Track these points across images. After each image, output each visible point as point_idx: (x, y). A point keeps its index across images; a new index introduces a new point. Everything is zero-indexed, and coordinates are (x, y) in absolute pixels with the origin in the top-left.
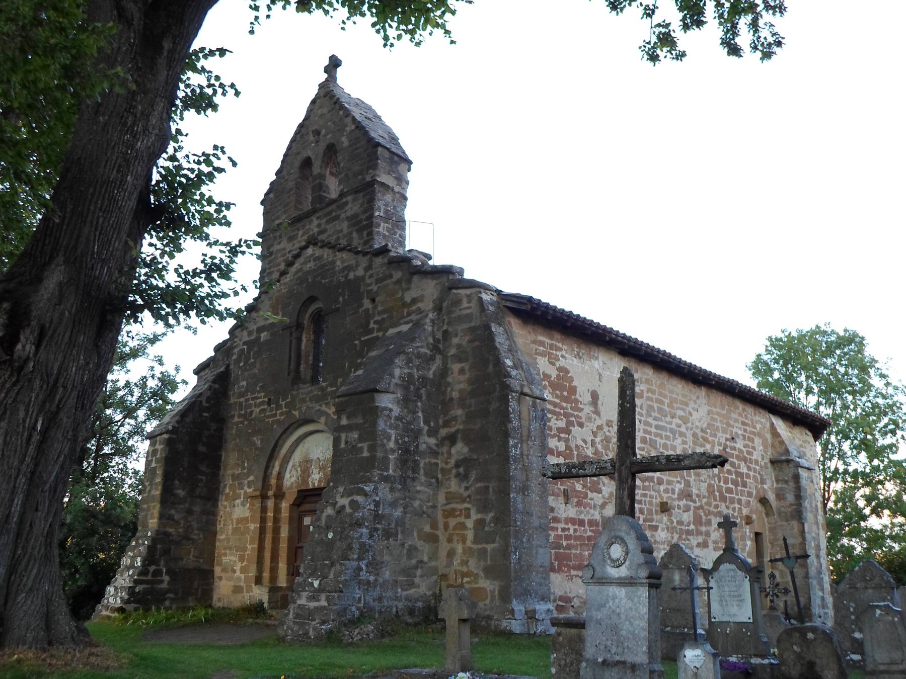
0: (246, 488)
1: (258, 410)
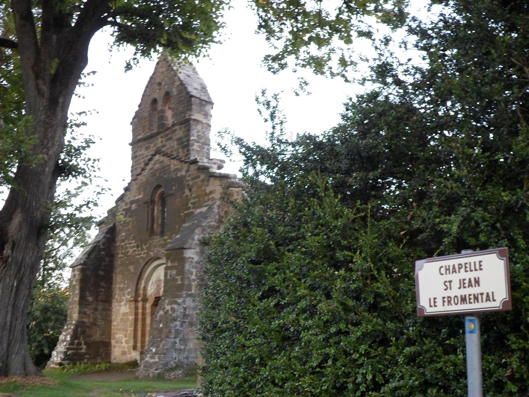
0: (126, 295)
1: (131, 250)
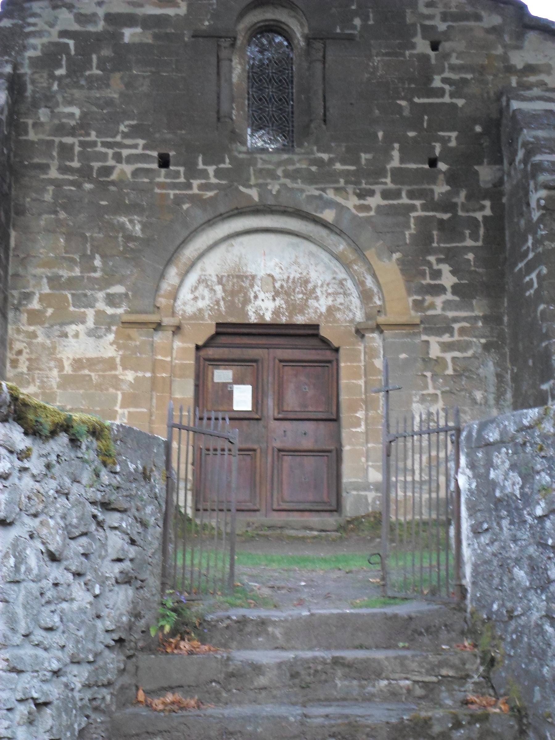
0: (101, 305)
1: (128, 169)
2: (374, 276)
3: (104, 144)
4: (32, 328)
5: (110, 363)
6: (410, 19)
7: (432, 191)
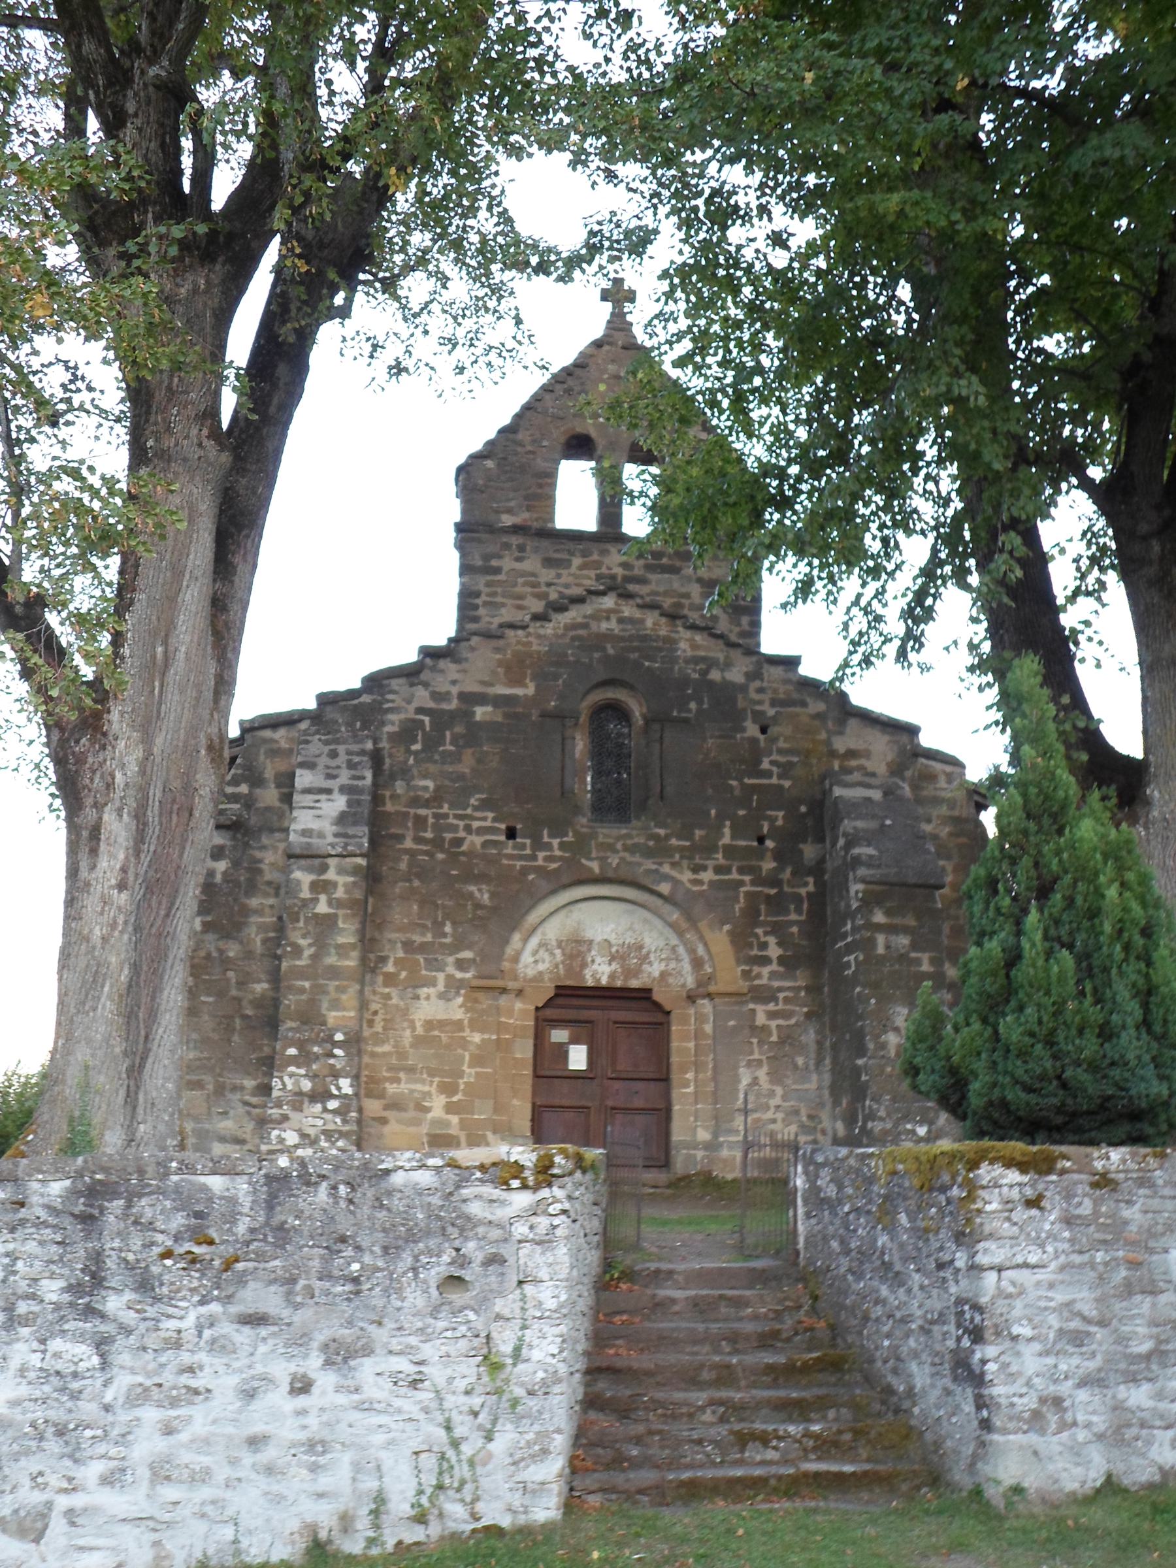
0: (450, 969)
1: (478, 840)
2: (706, 945)
3: (457, 817)
4: (387, 990)
5: (458, 1025)
6: (740, 704)
7: (760, 868)
